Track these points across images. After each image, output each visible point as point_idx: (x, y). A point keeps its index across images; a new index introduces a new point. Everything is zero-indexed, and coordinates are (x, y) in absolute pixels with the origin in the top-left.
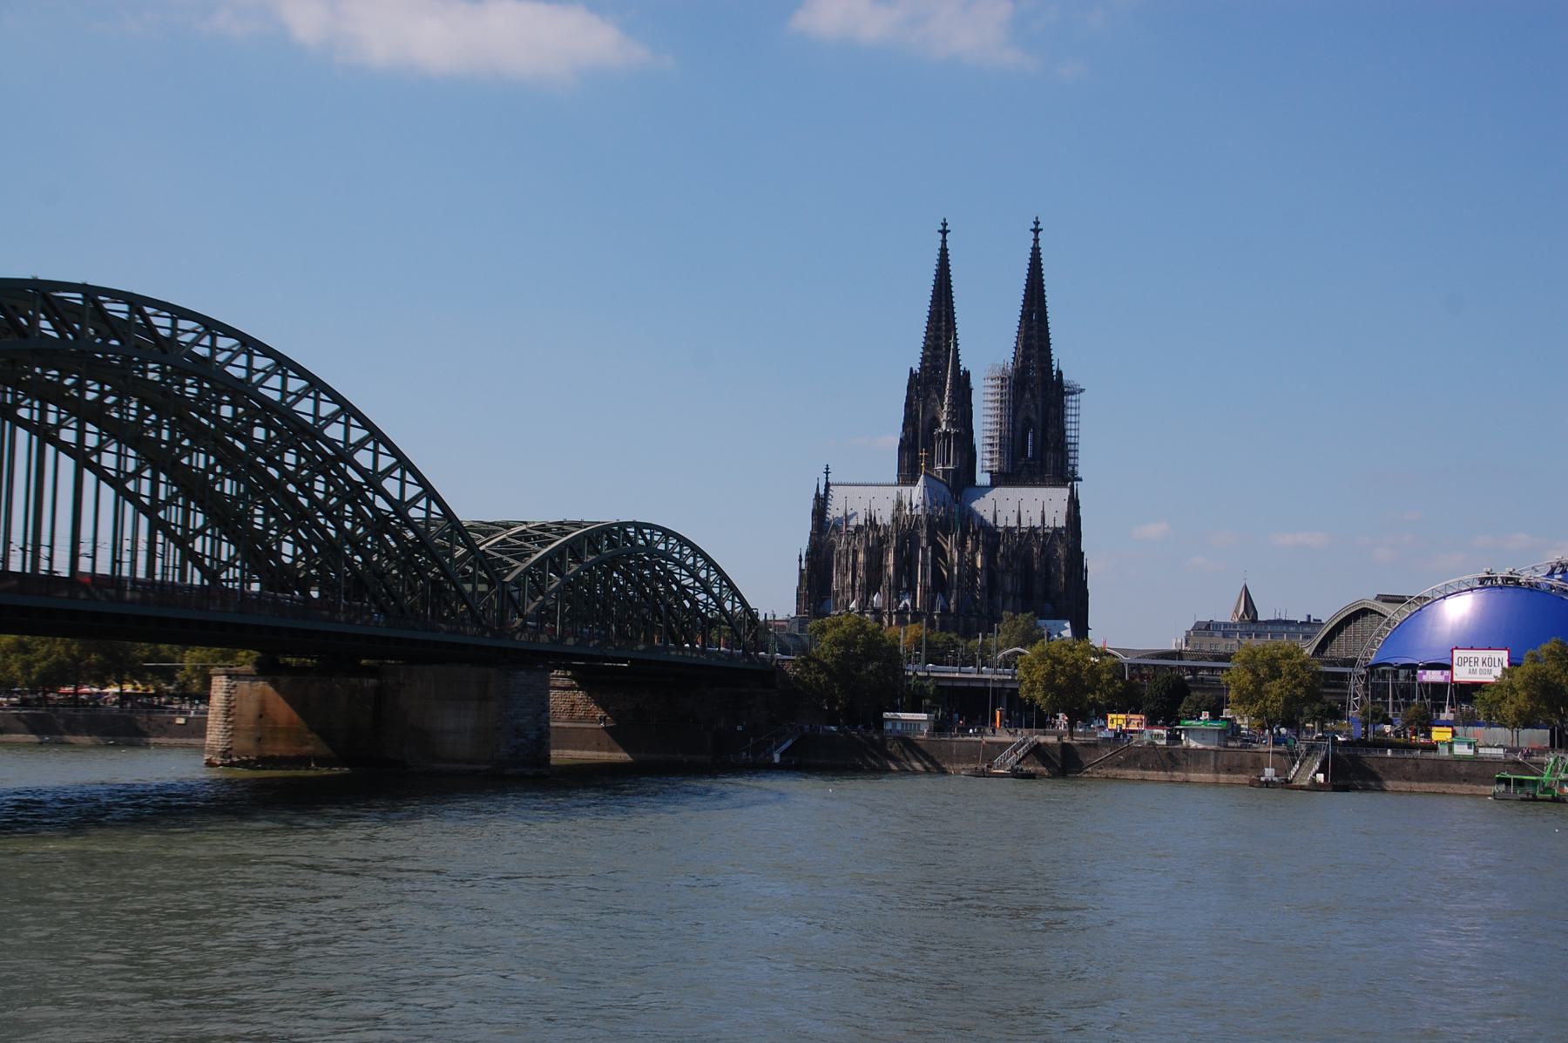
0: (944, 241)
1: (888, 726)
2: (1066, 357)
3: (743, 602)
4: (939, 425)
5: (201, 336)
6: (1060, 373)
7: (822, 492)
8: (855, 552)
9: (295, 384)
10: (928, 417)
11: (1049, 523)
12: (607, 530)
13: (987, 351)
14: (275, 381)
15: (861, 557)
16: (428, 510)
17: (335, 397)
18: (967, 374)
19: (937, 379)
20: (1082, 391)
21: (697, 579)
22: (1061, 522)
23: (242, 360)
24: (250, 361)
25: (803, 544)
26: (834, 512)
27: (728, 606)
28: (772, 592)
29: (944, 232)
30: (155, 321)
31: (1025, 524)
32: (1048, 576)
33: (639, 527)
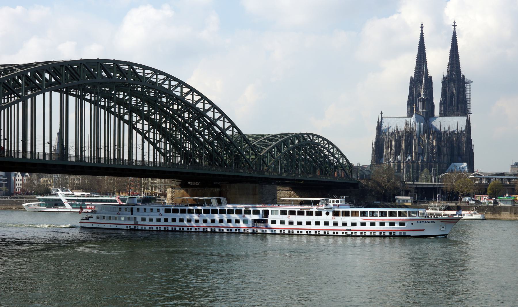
0: (422, 31)
1: (397, 201)
3: (347, 160)
4: (421, 96)
5: (153, 75)
6: (464, 76)
7: (380, 120)
8: (391, 141)
9: (185, 90)
10: (417, 93)
11: (460, 129)
14: (179, 89)
15: (393, 143)
16: (233, 131)
18: (431, 77)
19: (420, 79)
20: (471, 82)
21: (330, 152)
22: (464, 128)
23: (167, 82)
24: (169, 83)
25: (373, 139)
26: (384, 127)
27: (341, 161)
29: (422, 27)
30: (137, 71)
31: (451, 130)
32: (460, 147)
33: (308, 135)
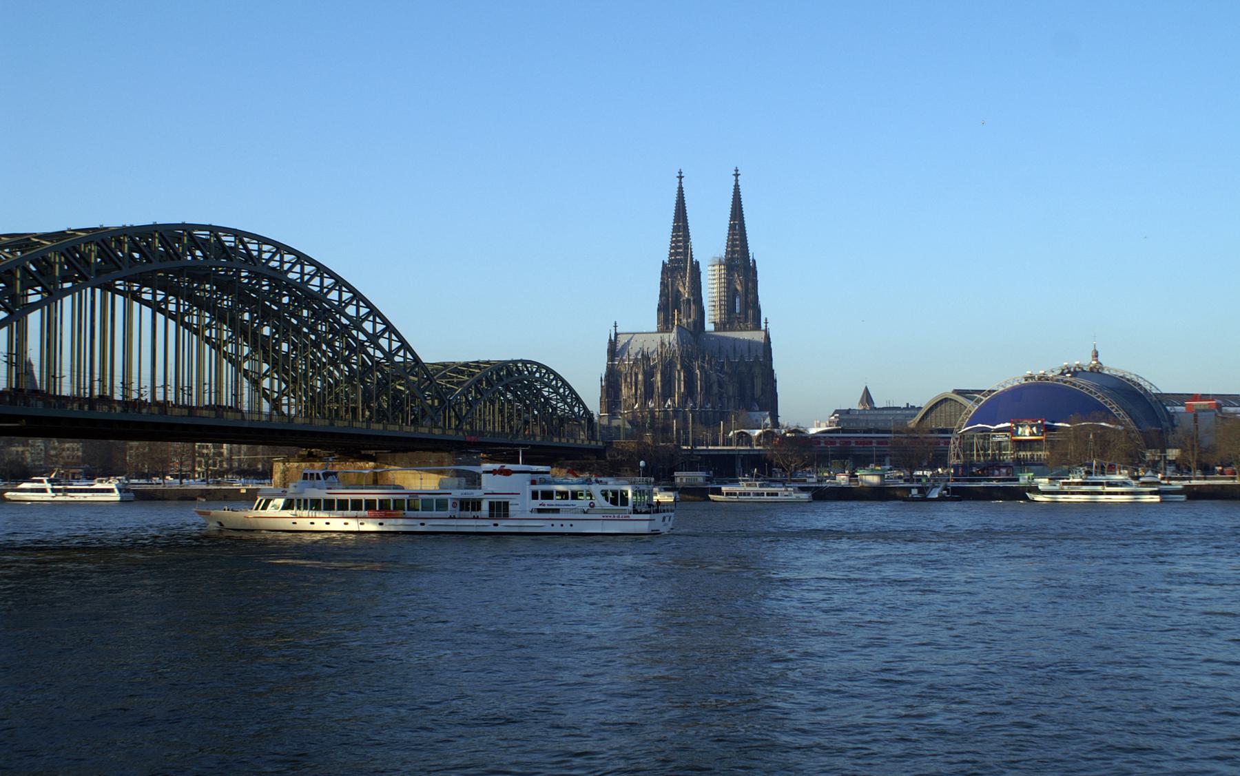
1: (678, 480)
2: (756, 249)
3: (585, 408)
5: (274, 254)
6: (754, 261)
8: (636, 375)
9: (328, 282)
12: (504, 364)
13: (709, 247)
14: (316, 281)
15: (640, 377)
16: (405, 357)
17: (351, 289)
18: (698, 263)
19: (679, 268)
21: (558, 394)
23: (297, 268)
24: (302, 269)
27: (576, 409)
28: (592, 397)
30: (250, 246)
33: (525, 362)
